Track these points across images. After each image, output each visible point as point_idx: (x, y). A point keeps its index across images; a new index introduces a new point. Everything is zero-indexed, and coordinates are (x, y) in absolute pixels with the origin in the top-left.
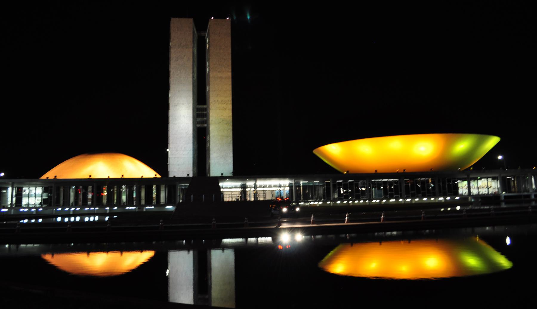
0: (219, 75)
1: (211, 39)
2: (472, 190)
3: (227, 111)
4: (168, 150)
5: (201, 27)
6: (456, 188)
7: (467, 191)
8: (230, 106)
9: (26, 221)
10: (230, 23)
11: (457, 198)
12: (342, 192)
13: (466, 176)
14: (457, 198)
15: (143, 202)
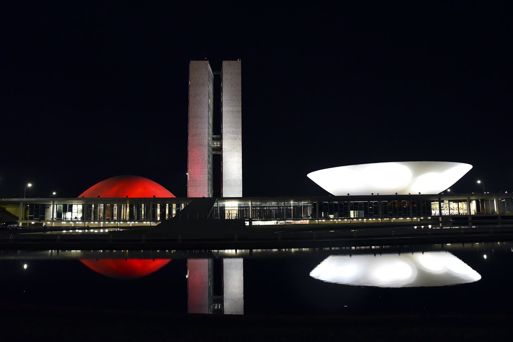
2: (442, 211)
5: (217, 69)
6: (429, 209)
8: (240, 136)
9: (64, 231)
11: (429, 218)
13: (438, 199)
14: (429, 218)
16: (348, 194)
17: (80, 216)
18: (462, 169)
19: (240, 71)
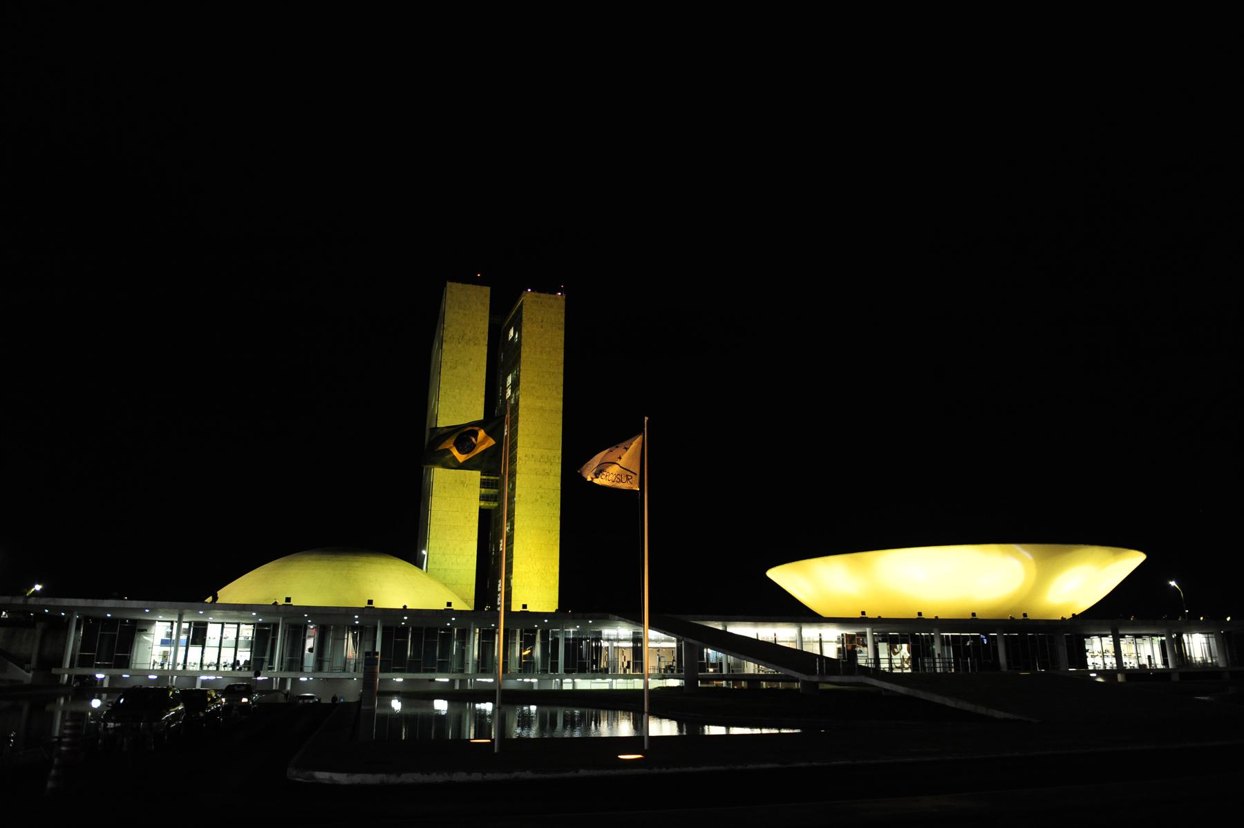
0: (539, 404)
1: (524, 330)
2: (1125, 660)
3: (552, 478)
4: (424, 552)
7: (1114, 661)
8: (557, 469)
10: (563, 304)
12: (712, 654)
15: (514, 666)
16: (920, 614)
17: (244, 656)
18: (1120, 565)
19: (563, 320)
